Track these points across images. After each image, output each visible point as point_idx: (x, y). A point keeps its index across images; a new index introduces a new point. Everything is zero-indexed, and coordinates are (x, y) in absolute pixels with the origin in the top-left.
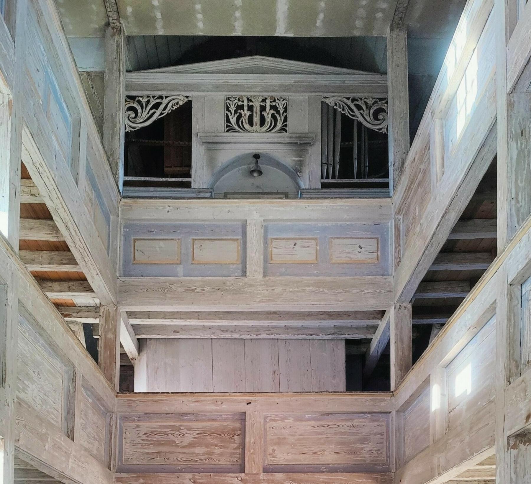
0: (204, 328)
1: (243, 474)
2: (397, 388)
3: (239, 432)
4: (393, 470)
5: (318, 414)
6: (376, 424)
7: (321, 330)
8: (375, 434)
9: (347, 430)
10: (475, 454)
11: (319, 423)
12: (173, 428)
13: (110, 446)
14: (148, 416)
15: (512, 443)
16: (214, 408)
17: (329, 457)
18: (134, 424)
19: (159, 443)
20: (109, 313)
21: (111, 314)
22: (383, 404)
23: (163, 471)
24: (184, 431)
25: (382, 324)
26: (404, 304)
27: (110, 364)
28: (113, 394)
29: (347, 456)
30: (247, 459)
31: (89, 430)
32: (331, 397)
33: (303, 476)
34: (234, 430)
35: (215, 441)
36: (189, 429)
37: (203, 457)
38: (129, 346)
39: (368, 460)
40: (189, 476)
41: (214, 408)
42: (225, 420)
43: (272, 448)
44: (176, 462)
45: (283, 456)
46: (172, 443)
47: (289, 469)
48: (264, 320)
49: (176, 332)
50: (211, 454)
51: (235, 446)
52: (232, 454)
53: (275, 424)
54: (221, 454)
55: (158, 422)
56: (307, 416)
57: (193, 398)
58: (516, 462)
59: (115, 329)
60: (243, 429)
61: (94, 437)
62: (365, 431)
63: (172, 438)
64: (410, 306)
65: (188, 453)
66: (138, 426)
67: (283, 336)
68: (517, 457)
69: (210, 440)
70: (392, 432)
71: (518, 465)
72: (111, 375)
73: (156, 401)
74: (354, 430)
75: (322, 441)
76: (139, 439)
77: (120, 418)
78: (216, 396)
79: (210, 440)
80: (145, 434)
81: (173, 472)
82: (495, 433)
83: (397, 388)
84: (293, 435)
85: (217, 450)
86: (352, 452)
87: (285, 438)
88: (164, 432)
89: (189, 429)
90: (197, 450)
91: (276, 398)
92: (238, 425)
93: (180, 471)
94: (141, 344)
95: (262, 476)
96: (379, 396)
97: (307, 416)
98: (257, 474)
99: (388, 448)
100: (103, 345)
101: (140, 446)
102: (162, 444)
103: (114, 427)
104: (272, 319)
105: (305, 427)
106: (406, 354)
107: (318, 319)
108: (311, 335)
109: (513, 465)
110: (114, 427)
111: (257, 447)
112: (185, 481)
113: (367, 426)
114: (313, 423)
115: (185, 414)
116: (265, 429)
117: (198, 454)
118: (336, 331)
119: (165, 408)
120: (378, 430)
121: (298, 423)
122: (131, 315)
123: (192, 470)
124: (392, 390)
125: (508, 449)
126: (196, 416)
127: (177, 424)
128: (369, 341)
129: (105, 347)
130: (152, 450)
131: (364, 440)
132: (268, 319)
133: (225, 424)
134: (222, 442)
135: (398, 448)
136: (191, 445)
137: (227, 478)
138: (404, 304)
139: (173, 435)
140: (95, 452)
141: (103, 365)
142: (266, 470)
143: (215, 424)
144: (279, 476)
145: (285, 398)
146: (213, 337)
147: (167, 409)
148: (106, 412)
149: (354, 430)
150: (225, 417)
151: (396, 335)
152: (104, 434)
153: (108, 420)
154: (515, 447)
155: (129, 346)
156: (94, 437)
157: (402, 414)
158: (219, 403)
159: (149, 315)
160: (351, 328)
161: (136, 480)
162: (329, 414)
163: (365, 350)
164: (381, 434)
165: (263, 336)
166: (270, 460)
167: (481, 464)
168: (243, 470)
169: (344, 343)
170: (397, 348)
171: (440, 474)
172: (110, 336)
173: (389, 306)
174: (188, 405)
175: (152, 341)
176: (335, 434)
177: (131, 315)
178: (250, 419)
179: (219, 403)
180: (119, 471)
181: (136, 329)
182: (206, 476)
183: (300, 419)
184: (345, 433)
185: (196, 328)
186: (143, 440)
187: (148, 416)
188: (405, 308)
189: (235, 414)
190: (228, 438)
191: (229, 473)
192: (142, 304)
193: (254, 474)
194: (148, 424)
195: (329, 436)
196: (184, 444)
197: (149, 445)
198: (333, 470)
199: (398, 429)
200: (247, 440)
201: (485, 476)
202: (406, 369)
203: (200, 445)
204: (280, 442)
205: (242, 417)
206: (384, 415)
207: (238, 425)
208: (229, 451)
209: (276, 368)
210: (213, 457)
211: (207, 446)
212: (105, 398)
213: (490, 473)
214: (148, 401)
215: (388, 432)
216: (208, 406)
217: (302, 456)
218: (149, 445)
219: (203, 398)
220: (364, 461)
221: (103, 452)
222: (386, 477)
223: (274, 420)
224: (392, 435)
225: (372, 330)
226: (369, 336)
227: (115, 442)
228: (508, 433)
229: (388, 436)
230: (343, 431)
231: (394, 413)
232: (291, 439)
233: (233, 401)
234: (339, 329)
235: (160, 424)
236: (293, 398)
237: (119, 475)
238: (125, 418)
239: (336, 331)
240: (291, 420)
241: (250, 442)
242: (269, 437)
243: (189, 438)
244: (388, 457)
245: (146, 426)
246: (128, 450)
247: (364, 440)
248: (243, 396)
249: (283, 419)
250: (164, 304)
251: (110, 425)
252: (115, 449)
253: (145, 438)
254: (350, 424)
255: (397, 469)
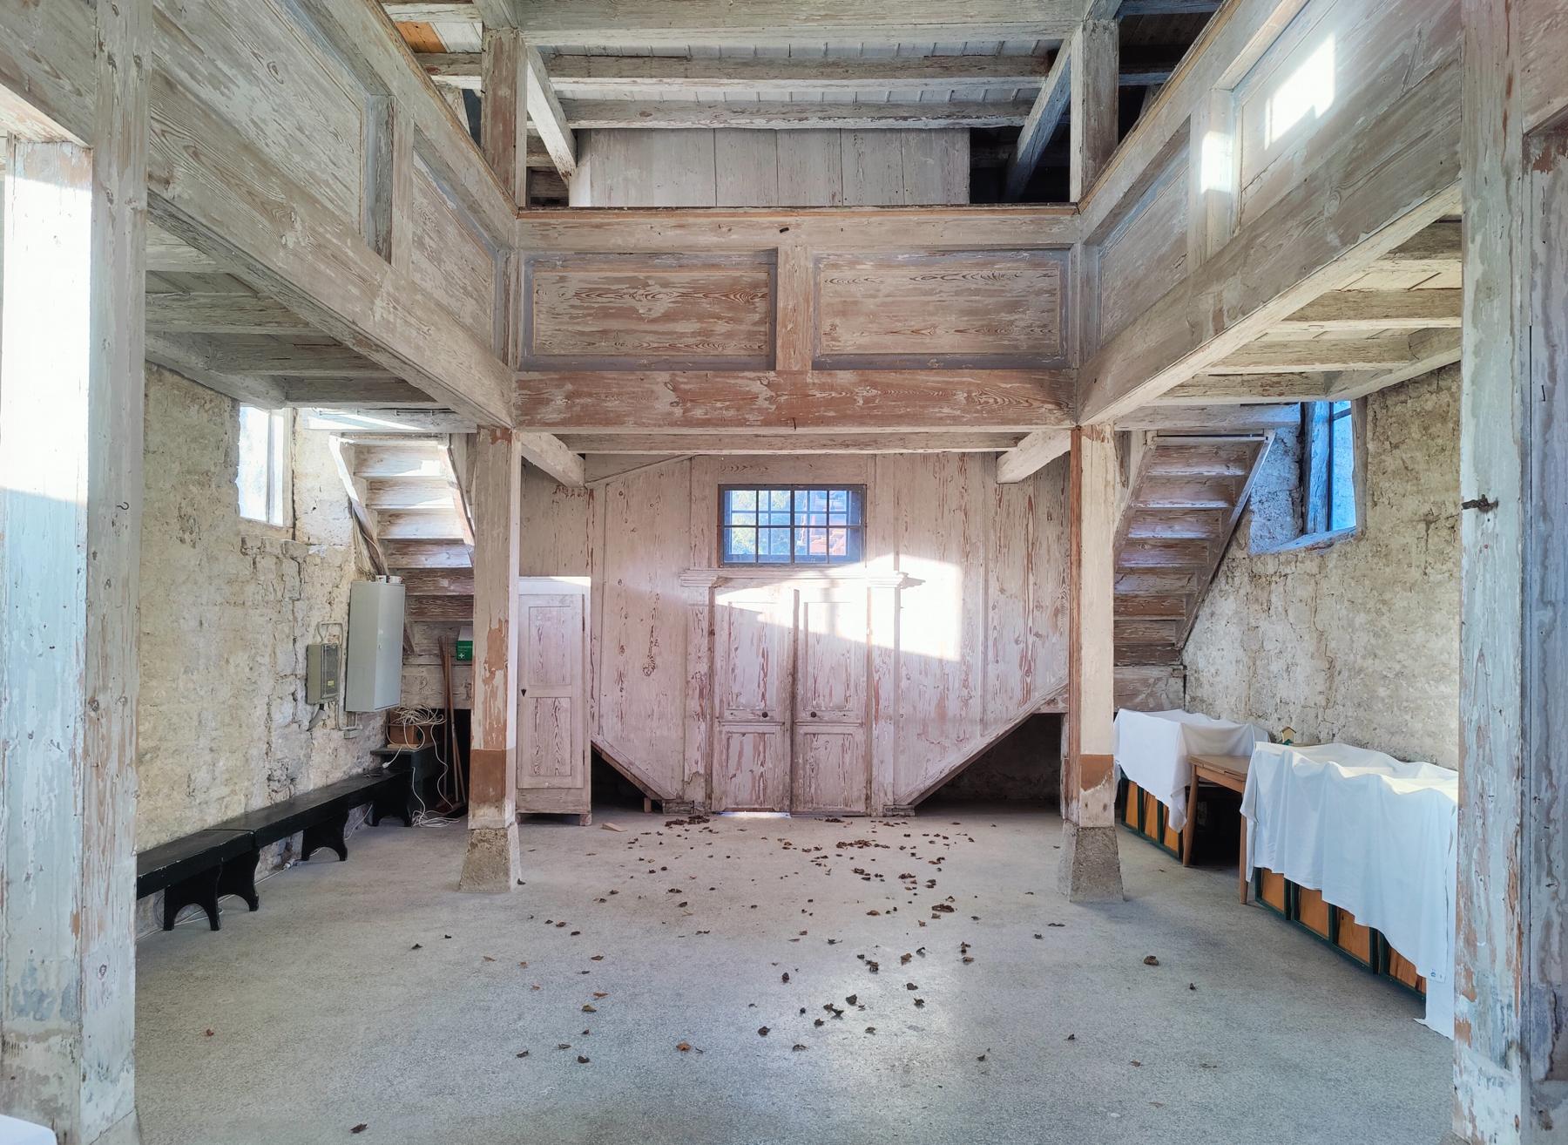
0: (699, 106)
1: (772, 373)
2: (1087, 191)
3: (765, 290)
4: (1076, 364)
5: (923, 253)
6: (1040, 272)
7: (924, 108)
8: (1039, 293)
9: (981, 284)
10: (1363, 236)
11: (925, 271)
12: (633, 283)
13: (506, 317)
14: (584, 256)
15: (1536, 152)
16: (715, 239)
17: (946, 341)
18: (555, 275)
19: (605, 313)
20: (502, 44)
21: (506, 47)
22: (1055, 230)
23: (614, 367)
24: (657, 289)
25: (1047, 86)
26: (1104, 22)
27: (505, 150)
28: (507, 208)
29: (981, 338)
30: (779, 342)
31: (449, 266)
32: (950, 216)
33: (892, 377)
34: (755, 285)
35: (716, 309)
36: (665, 284)
37: (691, 341)
38: (558, 147)
39: (1024, 347)
40: (664, 376)
41: (715, 239)
42: (737, 266)
43: (829, 322)
44: (638, 351)
45: (852, 339)
46: (630, 314)
47: (862, 363)
48: (816, 77)
49: (644, 114)
50: (707, 333)
51: (757, 317)
52: (751, 335)
53: (835, 274)
54: (729, 335)
55: (601, 270)
56: (900, 257)
57: (672, 221)
58: (1546, 207)
59: (514, 78)
60: (772, 283)
61: (464, 288)
62: (1020, 285)
63: (628, 301)
64: (1114, 26)
65: (663, 333)
66: (562, 279)
67: (851, 123)
68: (1550, 192)
69: (706, 305)
70: (1074, 287)
71: (1553, 219)
72: (507, 172)
73: (598, 226)
74: (997, 286)
75: (931, 308)
76: (565, 305)
77: (527, 263)
78: (717, 215)
79: (706, 305)
80: (577, 294)
81: (631, 369)
82: (1458, 147)
83: (1087, 191)
84: (874, 297)
85: (722, 327)
86: (993, 330)
87: (855, 303)
88: (615, 292)
89: (665, 284)
90: (681, 327)
91: (839, 221)
92: (763, 276)
93: (647, 367)
94: (580, 141)
95: (811, 377)
96: (1048, 212)
97: (900, 257)
98: (801, 373)
99: (1065, 321)
100: (489, 110)
101: (566, 318)
102: (613, 316)
103: (513, 279)
104: (829, 76)
105: (896, 280)
106: (1106, 123)
107: (920, 76)
108: (905, 119)
109: (1539, 214)
110: (513, 279)
111: (800, 319)
112: (655, 387)
113: (1024, 278)
114: (913, 272)
115: (655, 254)
116: (816, 284)
117: (682, 335)
118: (954, 110)
119: (616, 240)
120: (1044, 284)
121: (882, 272)
122: (556, 62)
123: (669, 366)
124: (1075, 192)
125: (1525, 171)
126: (679, 257)
127: (641, 275)
128: (1016, 131)
129: (495, 114)
130: (592, 326)
131: (1014, 306)
132: (823, 75)
133: (738, 274)
134: (731, 309)
135: (1087, 317)
136: (668, 317)
137: (739, 381)
138: (1104, 22)
139: (632, 295)
140: (468, 321)
141: (491, 151)
142: (818, 366)
143: (717, 275)
144: (845, 377)
145: (857, 219)
146: (716, 125)
147: (620, 242)
148: (497, 246)
149: (997, 286)
150: (735, 259)
151: (1086, 85)
152: (491, 291)
153: (501, 264)
154: (1544, 164)
155: (558, 147)
156: (464, 288)
157: (1096, 249)
158: (724, 229)
159: (591, 62)
160: (983, 105)
161: (559, 386)
162: (946, 251)
163: (1005, 156)
164: (1051, 292)
165: (813, 122)
166: (826, 347)
167: (1300, 316)
168: (771, 365)
169: (967, 136)
170: (1087, 114)
171: (1220, 330)
172: (504, 91)
173: (1070, 29)
174: (663, 234)
175: (601, 137)
176: (957, 293)
177: (556, 62)
178: (786, 262)
179: (724, 229)
180: (526, 367)
181: (568, 107)
182: (697, 377)
183: (886, 264)
184: (977, 292)
185: (683, 107)
186: (573, 307)
187: (584, 256)
188: (1105, 28)
189: (757, 253)
190: (741, 302)
191: (743, 370)
192: (569, 25)
193: (794, 373)
194: (582, 275)
195: (944, 296)
196: (654, 315)
197: (585, 316)
198: (952, 364)
199: (1087, 280)
200: (780, 304)
201: (1284, 363)
202: (1103, 154)
203: (686, 316)
204: (846, 309)
205: (770, 258)
206: (1058, 254)
207: (763, 276)
208: (743, 327)
209: (837, 188)
210: (712, 340)
211: (700, 317)
212: (486, 206)
213: (1294, 356)
214: (582, 226)
215: (1064, 287)
216: (703, 237)
217: (889, 339)
218: (585, 316)
219: (691, 220)
220: (1016, 347)
221: (489, 327)
222: (1061, 379)
223: (835, 266)
224: (1074, 293)
225: (1023, 109)
226: (1016, 121)
227: (517, 310)
228: (1531, 121)
229: (1064, 296)
230: (973, 286)
231: (1078, 247)
232: (870, 304)
233: (751, 226)
234: (958, 106)
235: (608, 274)
236: (873, 219)
237: (525, 376)
238: (536, 263)
239: (954, 110)
240: (868, 266)
241: (785, 308)
242: (824, 301)
243: (664, 303)
244: (1064, 339)
245: (578, 278)
246: (544, 327)
247: (1014, 306)
248: (771, 215)
249: (853, 264)
250: (611, 27)
251: (505, 273)
252: (516, 324)
253: (577, 303)
254: (986, 273)
255: (1083, 361)
